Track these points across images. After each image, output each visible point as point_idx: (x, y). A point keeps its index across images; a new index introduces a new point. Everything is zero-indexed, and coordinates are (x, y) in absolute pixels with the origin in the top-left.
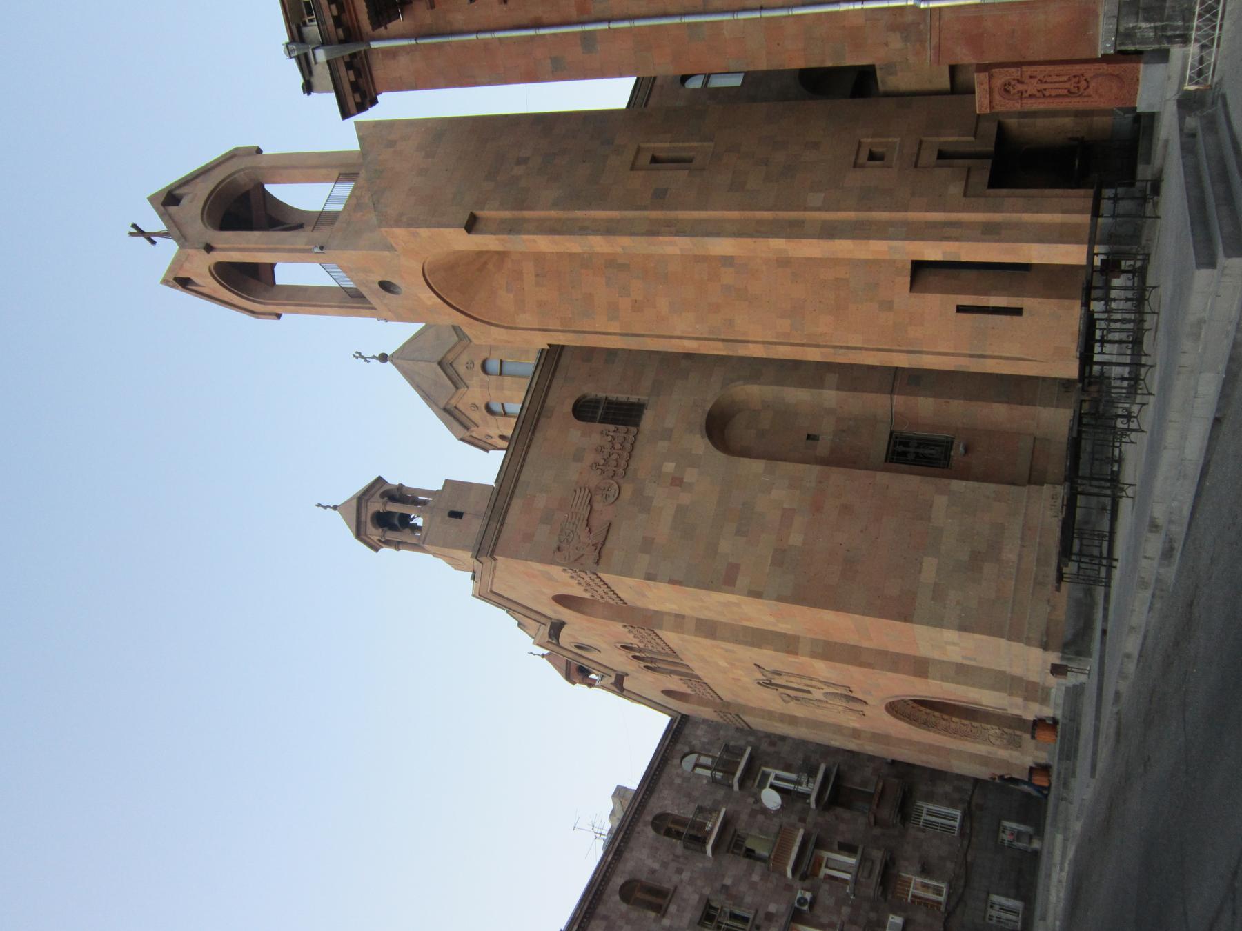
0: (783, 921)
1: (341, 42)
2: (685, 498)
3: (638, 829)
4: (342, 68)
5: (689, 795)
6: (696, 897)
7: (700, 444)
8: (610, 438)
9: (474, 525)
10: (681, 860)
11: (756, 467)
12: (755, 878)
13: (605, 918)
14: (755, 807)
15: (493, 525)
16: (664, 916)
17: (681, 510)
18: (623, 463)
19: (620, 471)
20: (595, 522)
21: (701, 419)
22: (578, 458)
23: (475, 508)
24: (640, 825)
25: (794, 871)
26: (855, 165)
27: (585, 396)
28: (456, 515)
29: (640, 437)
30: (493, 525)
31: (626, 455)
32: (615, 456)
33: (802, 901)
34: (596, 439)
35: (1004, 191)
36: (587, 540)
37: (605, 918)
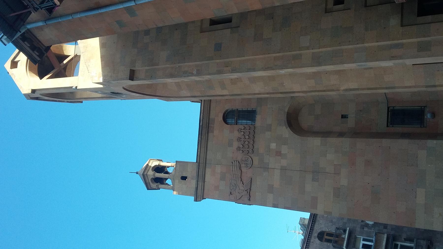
3: (312, 241)
5: (332, 221)
7: (286, 132)
8: (242, 133)
9: (192, 183)
11: (315, 142)
14: (362, 224)
15: (200, 184)
17: (283, 169)
19: (251, 151)
20: (245, 179)
21: (284, 117)
22: (230, 145)
23: (191, 173)
24: (313, 238)
26: (327, 11)
27: (227, 110)
28: (184, 178)
29: (256, 131)
30: (200, 184)
31: (252, 142)
32: (247, 143)
34: (236, 134)
35: (429, 18)
36: (242, 188)
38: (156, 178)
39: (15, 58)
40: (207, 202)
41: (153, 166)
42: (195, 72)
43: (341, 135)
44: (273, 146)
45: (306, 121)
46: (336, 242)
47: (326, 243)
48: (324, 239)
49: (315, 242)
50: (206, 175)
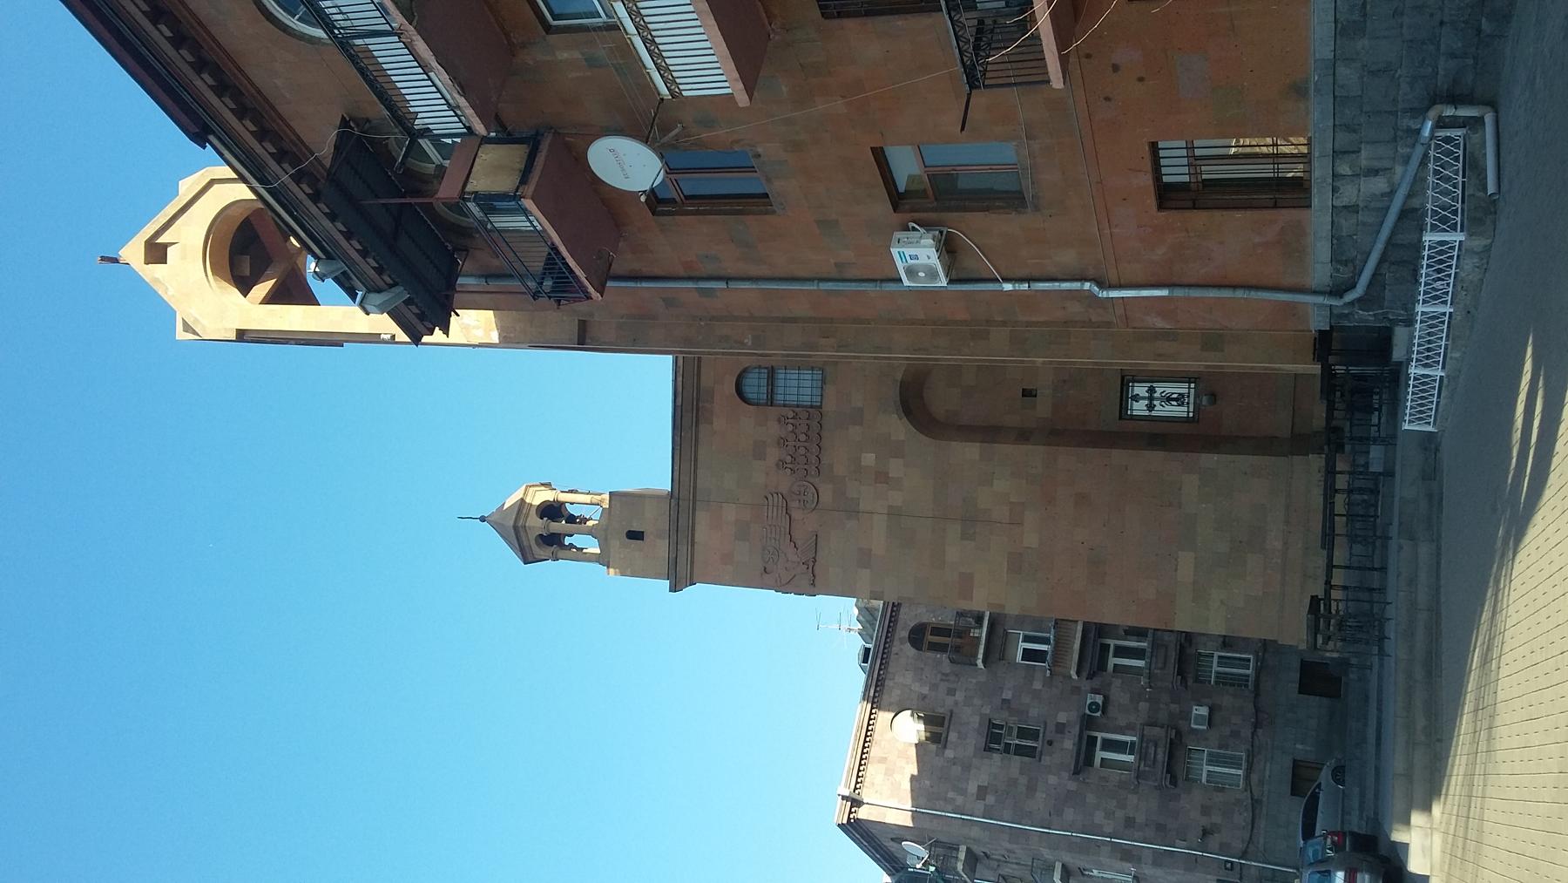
0: (1077, 728)
1: (391, 286)
2: (896, 498)
3: (894, 649)
4: (404, 310)
6: (977, 719)
7: (898, 428)
8: (790, 428)
9: (662, 548)
10: (952, 678)
11: (969, 451)
12: (1037, 685)
13: (883, 760)
15: (683, 549)
16: (945, 747)
17: (894, 513)
18: (813, 459)
19: (813, 471)
22: (759, 452)
23: (653, 521)
24: (896, 643)
25: (1078, 673)
28: (635, 535)
31: (815, 449)
33: (1094, 707)
34: (774, 429)
37: (883, 760)
38: (542, 533)
39: (158, 233)
40: (700, 593)
41: (537, 502)
42: (748, 341)
43: (1023, 436)
44: (869, 459)
45: (942, 399)
46: (957, 649)
47: (930, 654)
48: (925, 646)
49: (905, 651)
50: (697, 527)
